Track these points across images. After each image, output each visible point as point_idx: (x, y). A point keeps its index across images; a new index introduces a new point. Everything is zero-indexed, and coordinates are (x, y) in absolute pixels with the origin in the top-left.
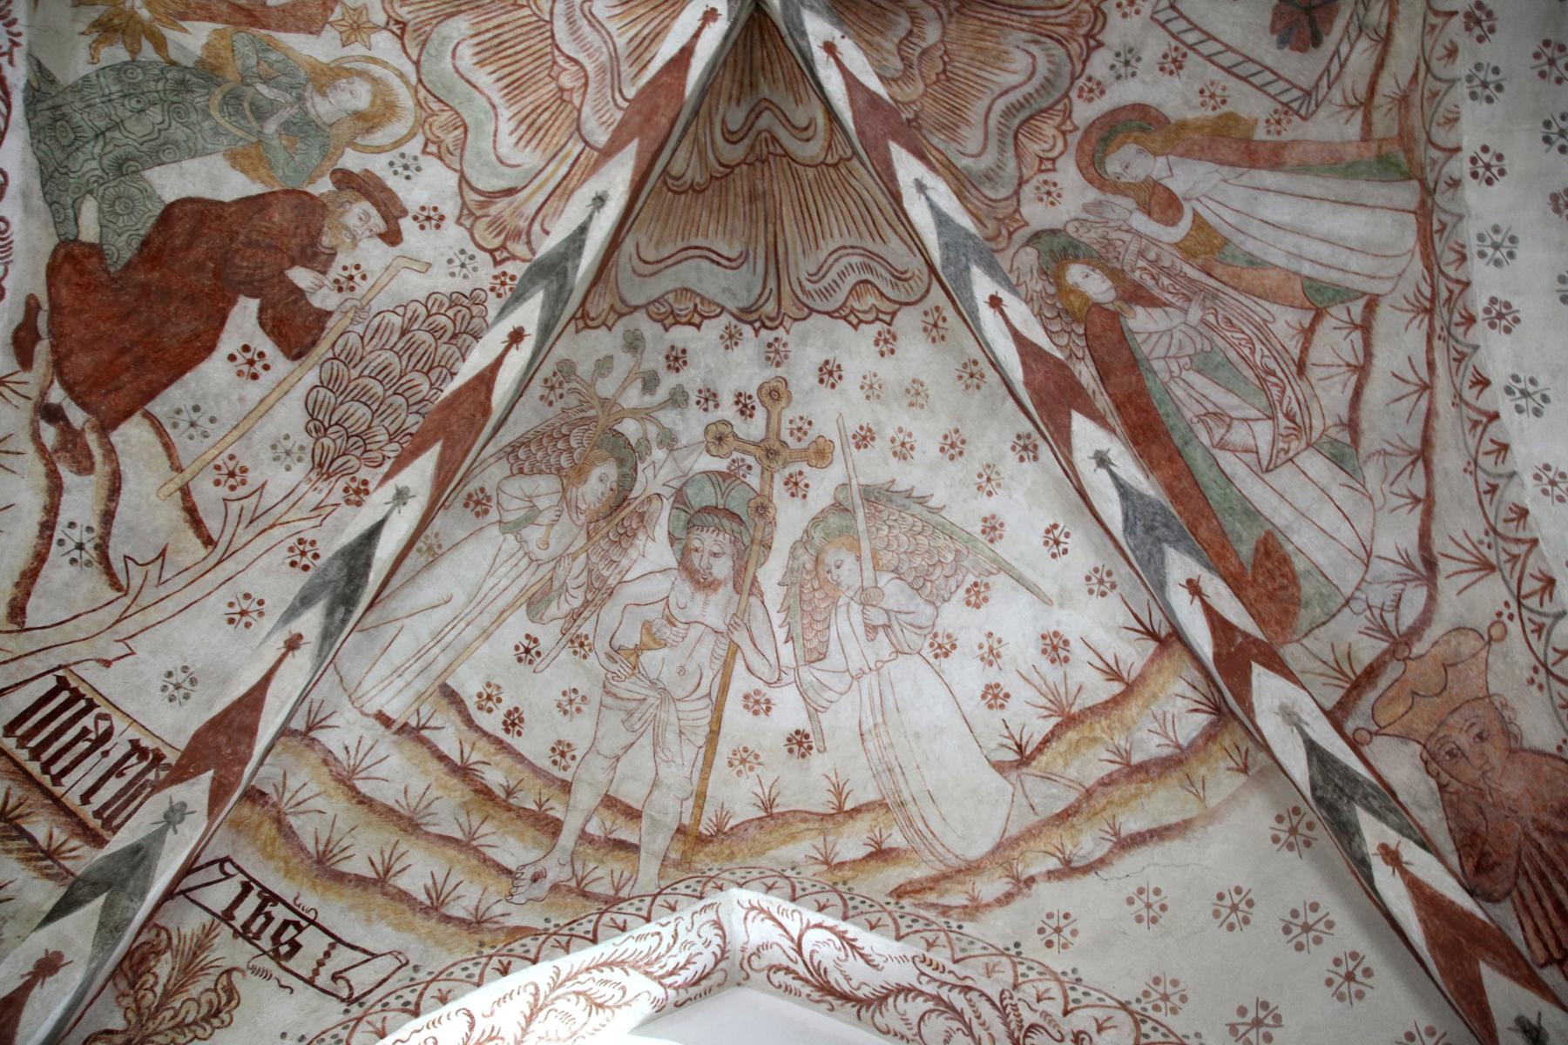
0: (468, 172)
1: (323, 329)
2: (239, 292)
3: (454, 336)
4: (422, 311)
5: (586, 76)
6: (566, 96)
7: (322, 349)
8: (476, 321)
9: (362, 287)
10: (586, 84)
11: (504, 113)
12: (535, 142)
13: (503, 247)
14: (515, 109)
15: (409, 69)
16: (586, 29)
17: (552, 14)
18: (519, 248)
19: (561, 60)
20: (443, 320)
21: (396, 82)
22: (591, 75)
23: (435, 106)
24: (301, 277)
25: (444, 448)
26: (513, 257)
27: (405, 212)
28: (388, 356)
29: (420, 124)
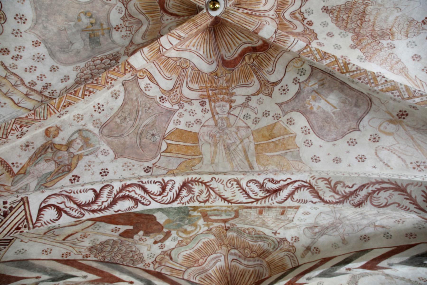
0: (175, 249)
1: (128, 238)
2: (134, 226)
3: (132, 260)
4: (137, 253)
5: (202, 265)
6: (197, 262)
7: (123, 239)
8: (137, 263)
9: (142, 242)
10: (200, 266)
11: (191, 251)
12: (184, 259)
13: (157, 262)
14: (193, 253)
15: (200, 232)
16: (213, 262)
17: (217, 253)
18: (157, 265)
19: (206, 258)
20: (136, 257)
21: (196, 232)
22: (202, 266)
23: (191, 239)
24: (141, 233)
25: (100, 279)
26: (154, 265)
27: (163, 242)
28: (125, 250)
29: (186, 238)
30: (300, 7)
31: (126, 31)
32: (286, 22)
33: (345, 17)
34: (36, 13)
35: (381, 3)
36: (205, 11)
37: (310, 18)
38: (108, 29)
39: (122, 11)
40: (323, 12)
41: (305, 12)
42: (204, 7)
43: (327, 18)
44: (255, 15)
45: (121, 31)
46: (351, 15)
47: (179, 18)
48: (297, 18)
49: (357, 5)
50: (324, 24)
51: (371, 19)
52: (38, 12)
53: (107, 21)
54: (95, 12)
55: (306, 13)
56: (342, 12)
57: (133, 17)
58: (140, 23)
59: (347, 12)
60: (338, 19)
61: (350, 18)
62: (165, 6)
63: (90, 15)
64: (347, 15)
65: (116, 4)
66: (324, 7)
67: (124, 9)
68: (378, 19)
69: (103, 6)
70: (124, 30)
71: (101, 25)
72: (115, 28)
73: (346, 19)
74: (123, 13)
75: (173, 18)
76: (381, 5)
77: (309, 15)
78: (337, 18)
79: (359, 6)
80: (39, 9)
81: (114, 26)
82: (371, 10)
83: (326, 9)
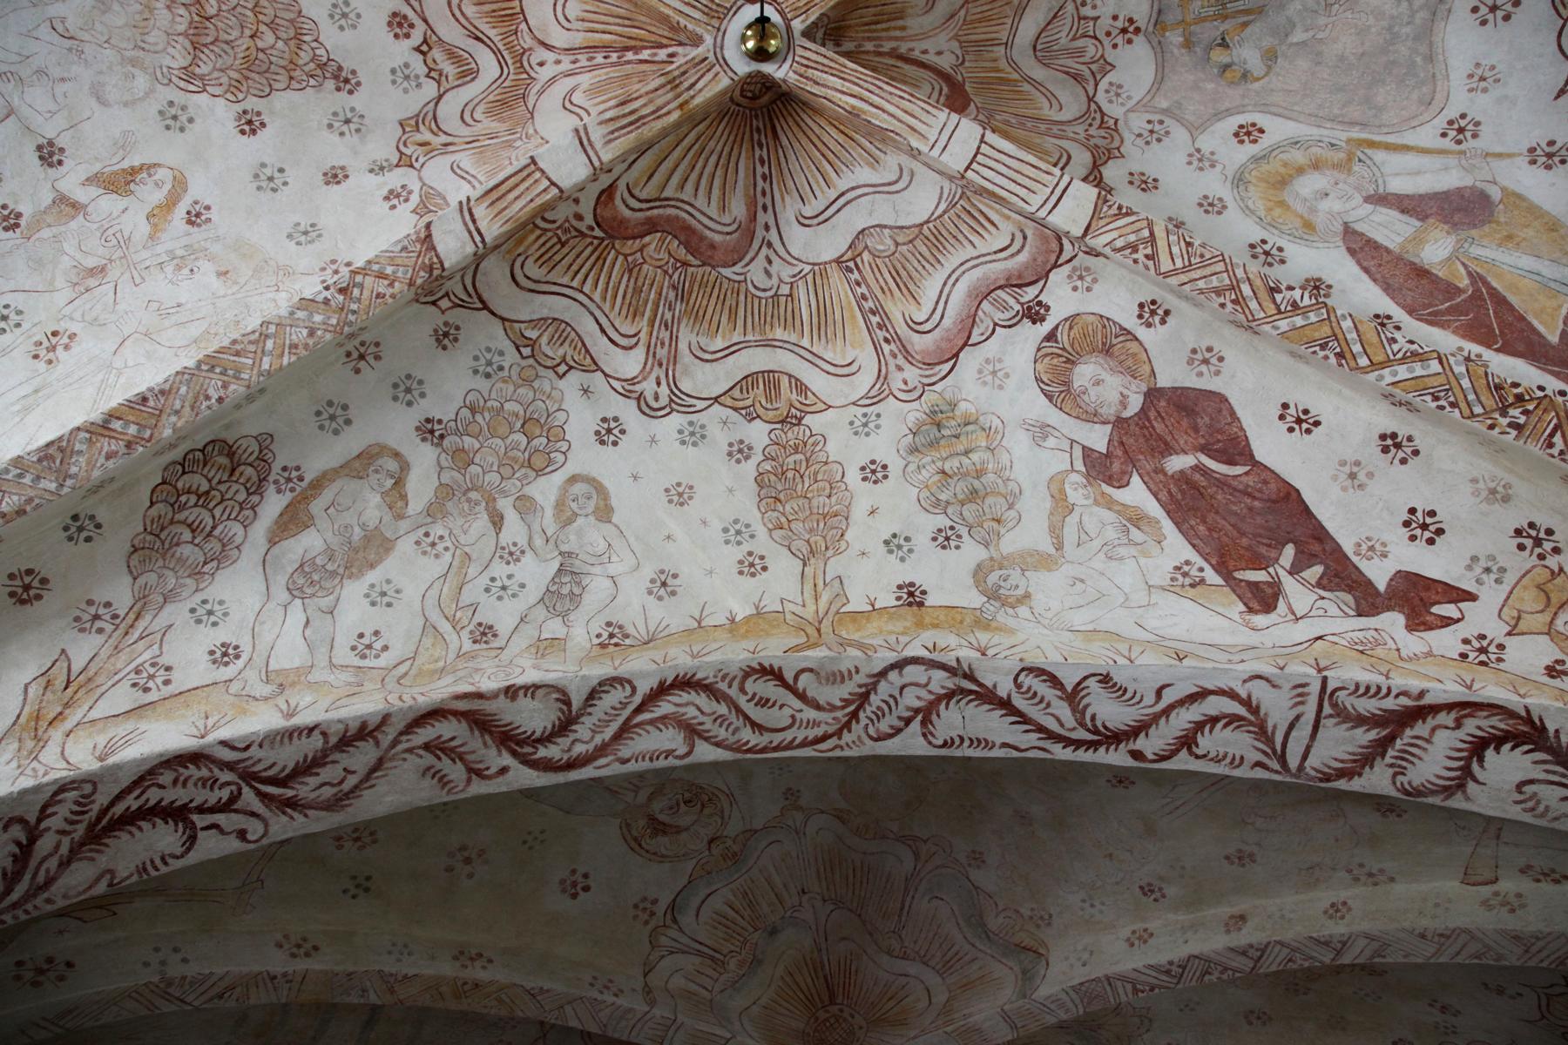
30: (440, 97)
31: (1096, 19)
32: (492, 33)
33: (268, 38)
34: (1431, 44)
35: (136, 72)
36: (798, 25)
37: (402, 51)
38: (1164, 29)
39: (1107, 91)
40: (354, 72)
41: (423, 79)
42: (800, 40)
43: (333, 40)
44: (606, 47)
45: (1115, 18)
46: (246, 42)
47: (894, 49)
48: (452, 54)
49: (225, 80)
50: (344, 15)
51: (169, 16)
52: (1423, 49)
53: (1168, 56)
54: (1210, 86)
55: (417, 77)
56: (283, 63)
57: (1067, 73)
58: (1041, 50)
59: (261, 55)
60: (292, 33)
61: (248, 32)
62: (945, 90)
63: (1228, 74)
64: (260, 44)
65: (1130, 110)
66: (350, 92)
67: (1101, 97)
68: (139, 7)
69: (1179, 105)
70: (1105, 23)
71: (1188, 44)
72: (1137, 30)
73: (263, 28)
74: (1103, 85)
75: (917, 53)
76: (134, 62)
77: (407, 65)
78: (298, 36)
79: (216, 74)
80: (1418, 59)
81: (1139, 40)
82: (170, 50)
83: (345, 81)
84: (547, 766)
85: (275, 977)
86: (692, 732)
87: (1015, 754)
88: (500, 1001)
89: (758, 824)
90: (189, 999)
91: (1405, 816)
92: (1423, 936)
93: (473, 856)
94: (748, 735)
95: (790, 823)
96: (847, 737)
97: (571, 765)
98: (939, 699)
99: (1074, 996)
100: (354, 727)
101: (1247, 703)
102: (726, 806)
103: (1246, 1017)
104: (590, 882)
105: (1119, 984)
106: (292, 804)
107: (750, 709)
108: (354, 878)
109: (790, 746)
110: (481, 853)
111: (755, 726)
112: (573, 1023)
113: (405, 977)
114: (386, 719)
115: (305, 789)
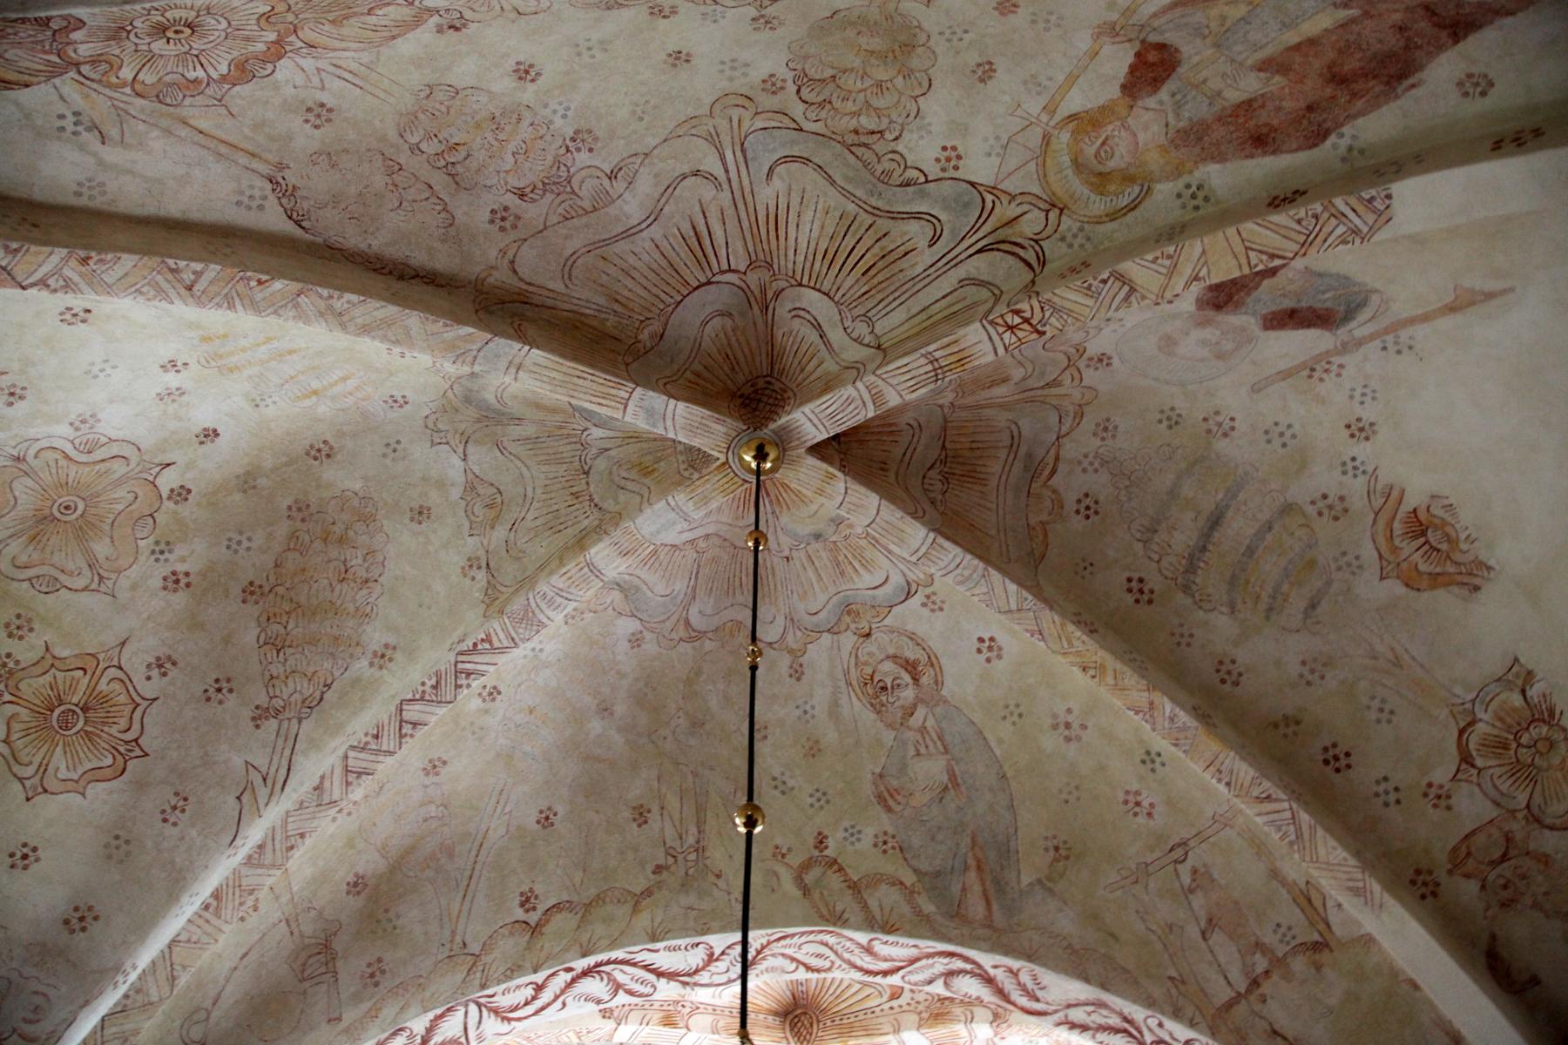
84: (966, 959)
85: (1228, 784)
86: (868, 950)
87: (649, 946)
88: (1071, 644)
89: (826, 638)
90: (1288, 814)
91: (345, 887)
92: (302, 836)
93: (1062, 727)
94: (831, 940)
95: (799, 633)
96: (764, 941)
97: (951, 954)
98: (703, 969)
99: (541, 617)
100: (1077, 1031)
101: (509, 1020)
102: (853, 670)
103: (331, 448)
104: (977, 645)
105: (506, 644)
106: (1126, 1020)
107: (827, 952)
108: (1153, 770)
109: (803, 934)
110: (1055, 727)
111: (826, 945)
112: (1012, 587)
113: (1137, 713)
114: (1059, 1024)
115: (1115, 1021)
